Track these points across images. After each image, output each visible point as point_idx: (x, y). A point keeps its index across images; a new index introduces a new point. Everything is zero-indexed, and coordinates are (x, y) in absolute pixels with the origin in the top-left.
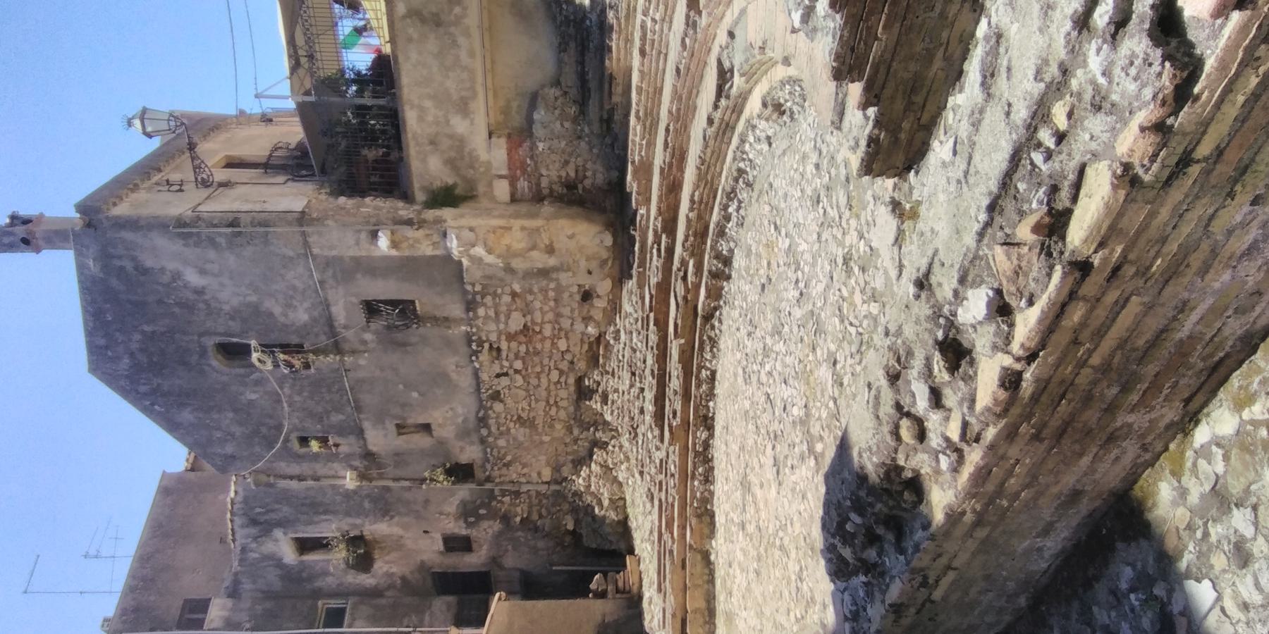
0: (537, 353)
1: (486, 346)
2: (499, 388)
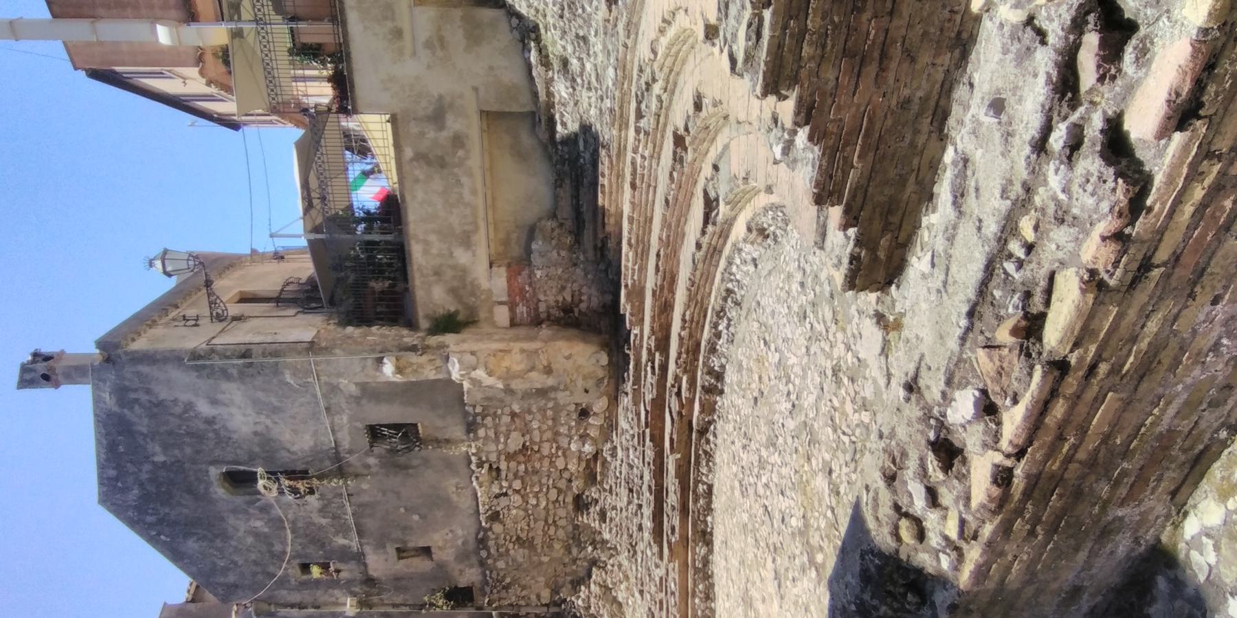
0: (536, 472)
1: (486, 466)
2: (498, 509)
